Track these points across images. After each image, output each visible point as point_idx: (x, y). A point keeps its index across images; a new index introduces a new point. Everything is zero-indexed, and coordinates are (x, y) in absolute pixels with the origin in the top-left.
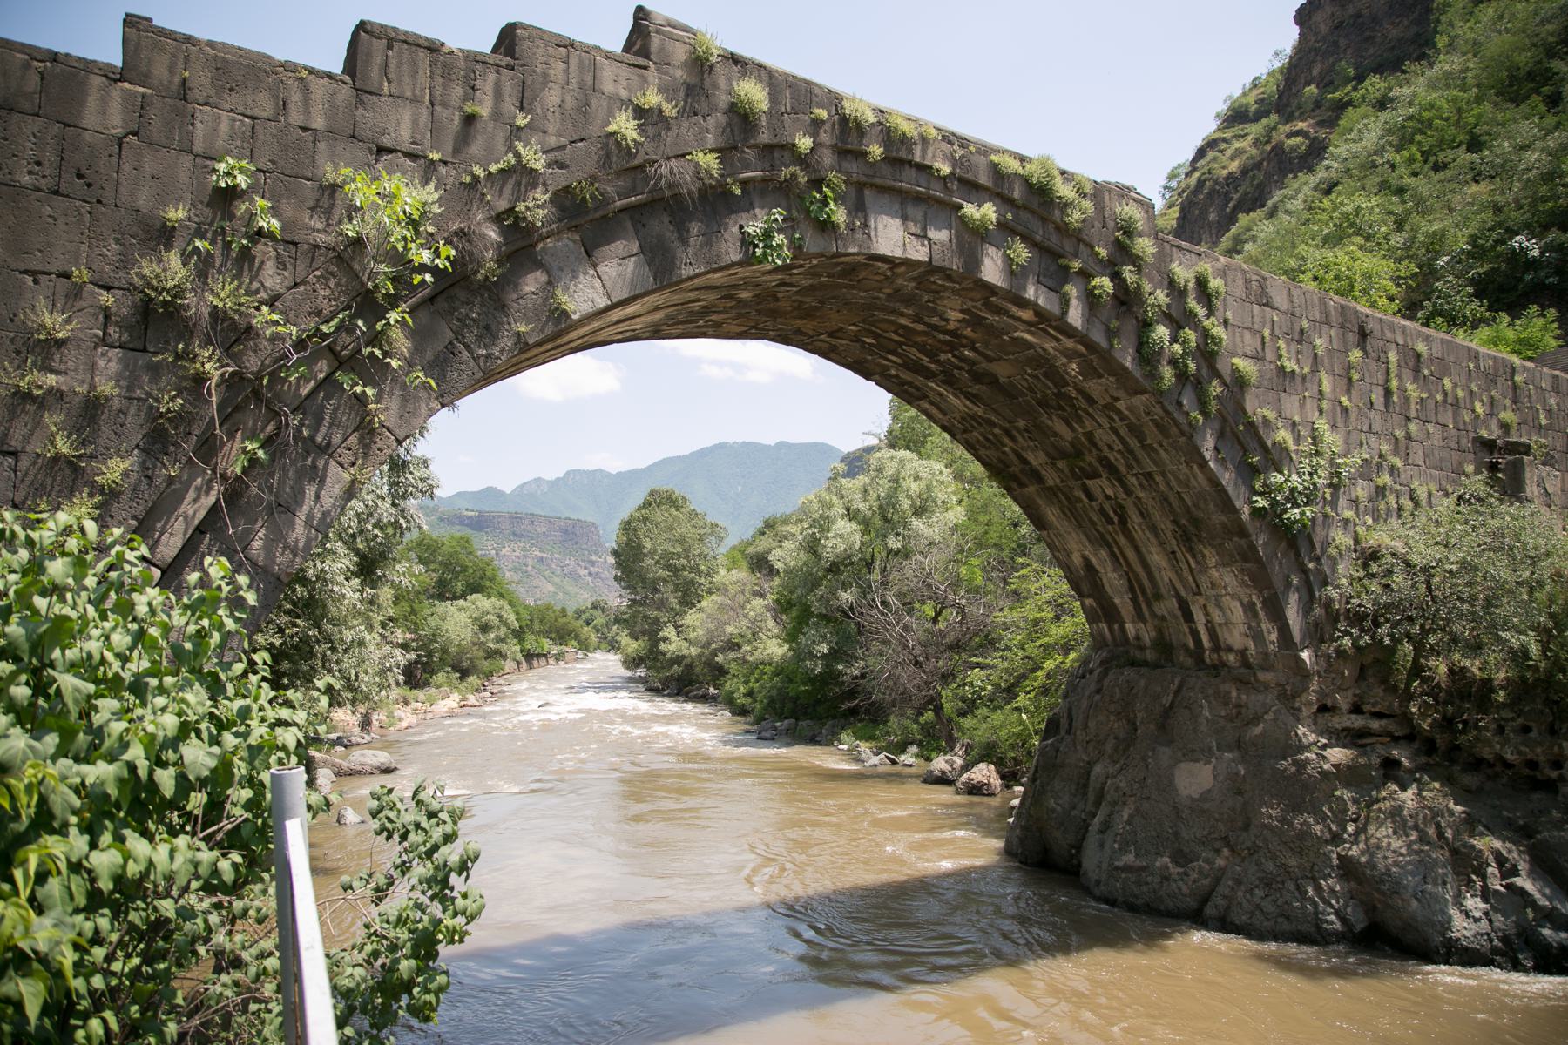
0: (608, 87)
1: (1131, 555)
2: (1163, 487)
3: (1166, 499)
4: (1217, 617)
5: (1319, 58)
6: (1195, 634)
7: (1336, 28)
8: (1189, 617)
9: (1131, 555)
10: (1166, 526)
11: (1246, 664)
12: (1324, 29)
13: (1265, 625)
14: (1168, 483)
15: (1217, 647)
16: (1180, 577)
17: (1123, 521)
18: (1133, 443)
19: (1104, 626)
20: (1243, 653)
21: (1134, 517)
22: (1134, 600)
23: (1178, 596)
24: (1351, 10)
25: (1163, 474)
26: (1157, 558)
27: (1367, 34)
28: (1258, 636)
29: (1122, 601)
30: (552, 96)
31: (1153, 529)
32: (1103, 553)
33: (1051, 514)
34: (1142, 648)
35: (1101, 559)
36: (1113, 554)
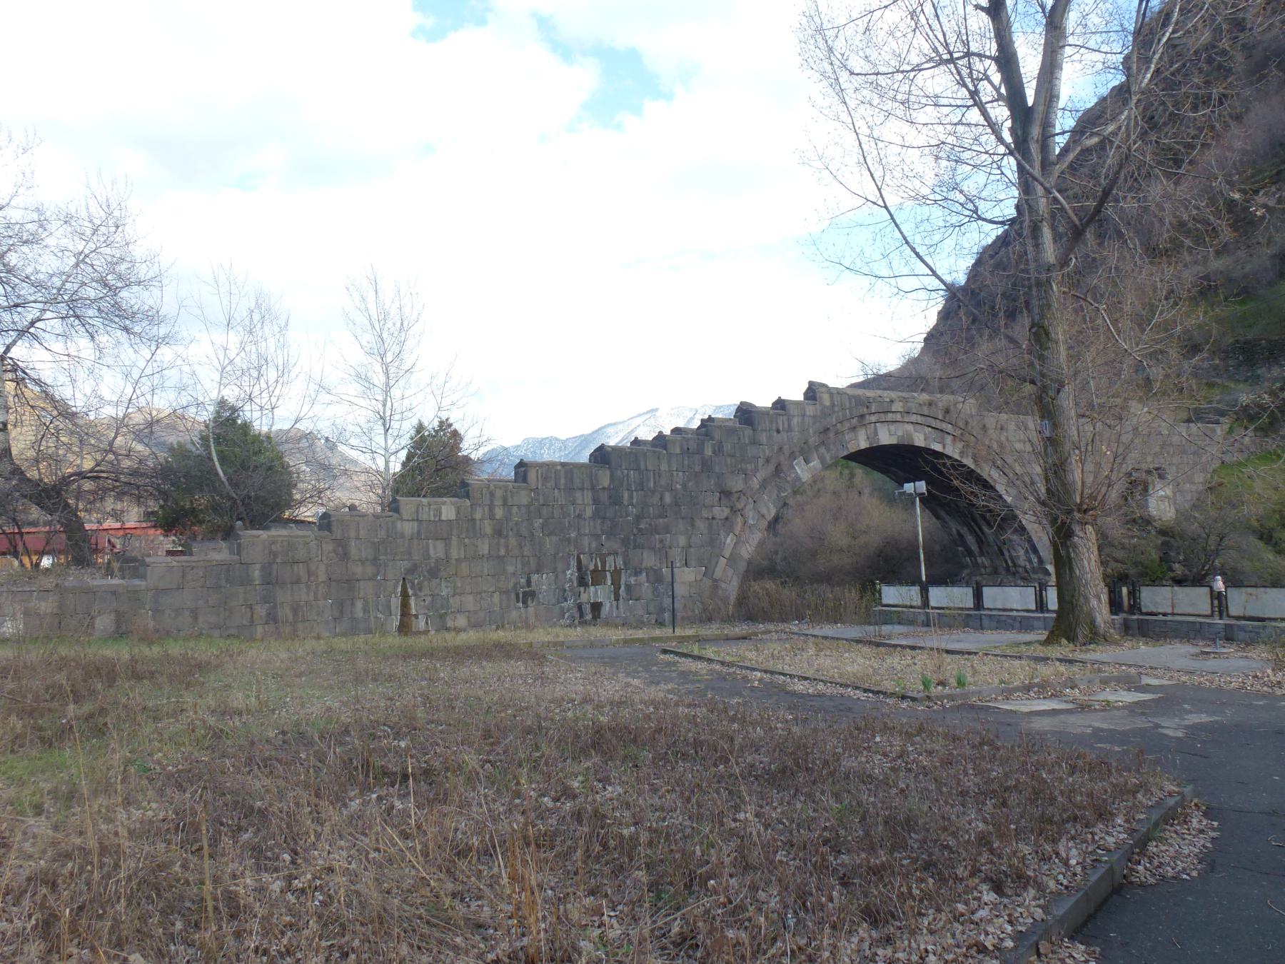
0: (808, 413)
1: (977, 529)
4: (1014, 554)
6: (1006, 562)
8: (1002, 554)
9: (977, 529)
11: (1026, 571)
13: (1032, 556)
15: (1015, 566)
19: (968, 559)
20: (1025, 568)
22: (979, 547)
26: (986, 529)
28: (1030, 561)
29: (974, 547)
30: (795, 421)
32: (966, 529)
33: (943, 514)
34: (985, 567)
35: (964, 531)
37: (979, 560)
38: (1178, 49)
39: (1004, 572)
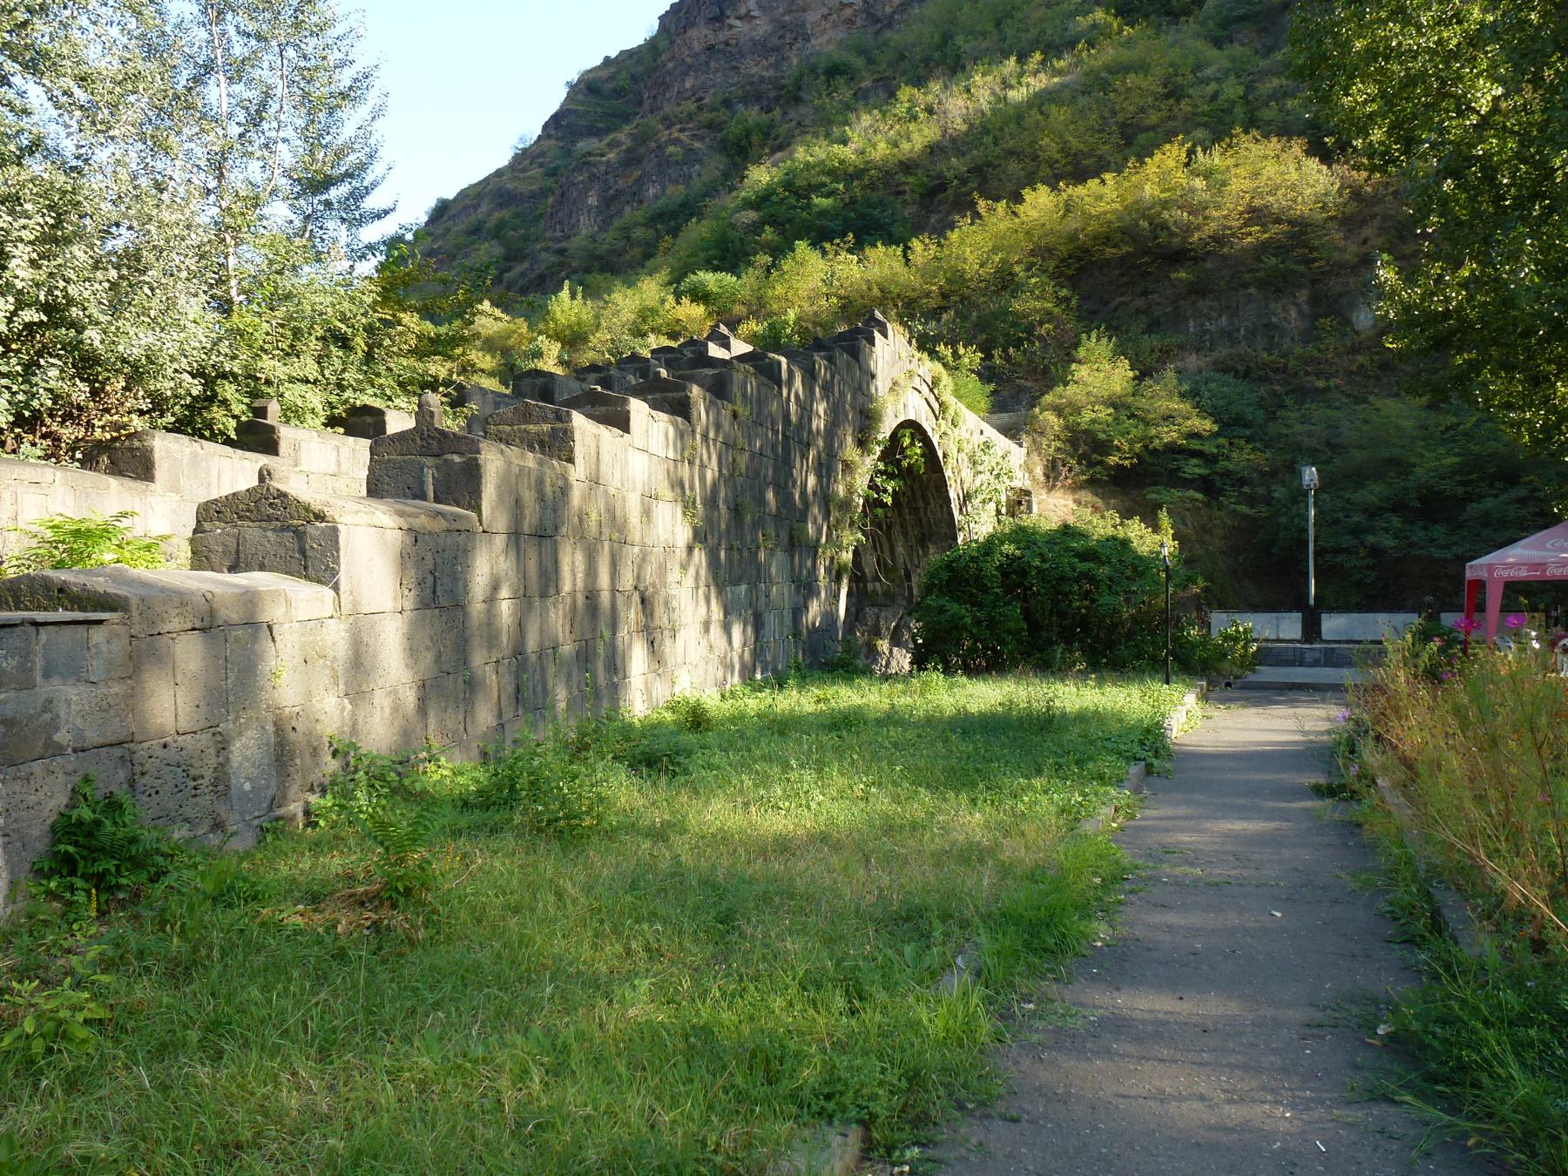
1: (886, 546)
2: (922, 515)
3: (920, 520)
5: (692, 73)
6: (910, 589)
7: (708, 49)
8: (908, 578)
10: (913, 532)
12: (697, 47)
14: (926, 514)
16: (911, 560)
17: (889, 527)
18: (918, 494)
21: (896, 530)
23: (906, 569)
24: (721, 38)
25: (926, 509)
27: (734, 64)
31: (905, 534)
36: (875, 546)
37: (870, 587)
38: (734, 31)
39: (904, 603)
